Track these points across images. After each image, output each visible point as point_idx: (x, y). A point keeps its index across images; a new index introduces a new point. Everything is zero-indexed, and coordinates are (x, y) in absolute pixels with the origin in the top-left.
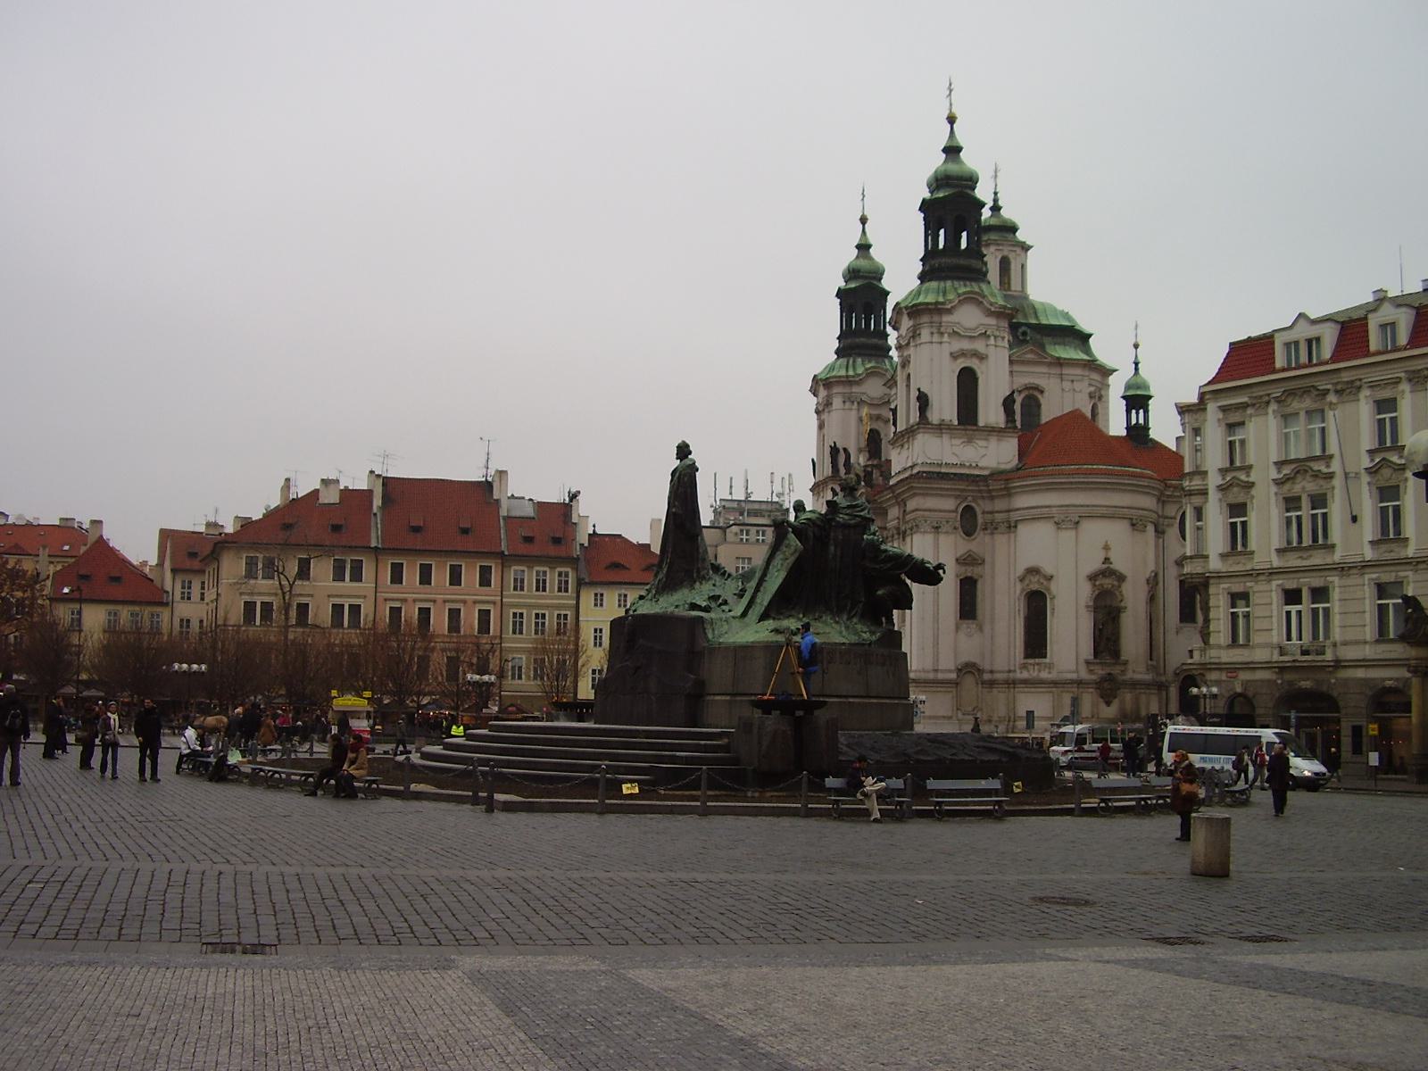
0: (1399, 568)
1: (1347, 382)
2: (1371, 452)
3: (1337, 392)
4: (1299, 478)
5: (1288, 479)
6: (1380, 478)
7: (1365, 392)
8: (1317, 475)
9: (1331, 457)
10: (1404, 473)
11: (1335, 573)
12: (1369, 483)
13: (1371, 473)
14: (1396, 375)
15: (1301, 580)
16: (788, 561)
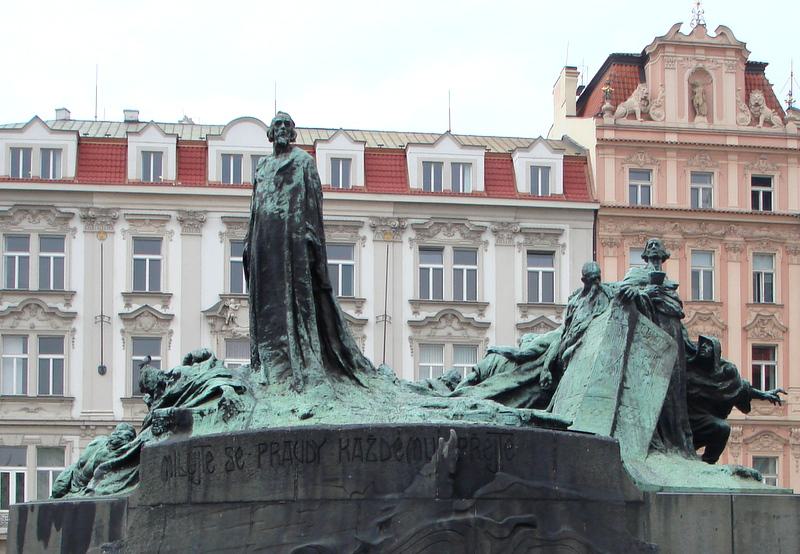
0: (64, 431)
1: (102, 210)
2: (125, 295)
3: (85, 218)
4: (27, 313)
5: (12, 312)
6: (138, 327)
7: (121, 226)
8: (52, 313)
9: (73, 294)
10: (168, 326)
11: (76, 431)
12: (123, 331)
13: (125, 320)
14: (165, 213)
15: (26, 437)
16: (662, 361)
